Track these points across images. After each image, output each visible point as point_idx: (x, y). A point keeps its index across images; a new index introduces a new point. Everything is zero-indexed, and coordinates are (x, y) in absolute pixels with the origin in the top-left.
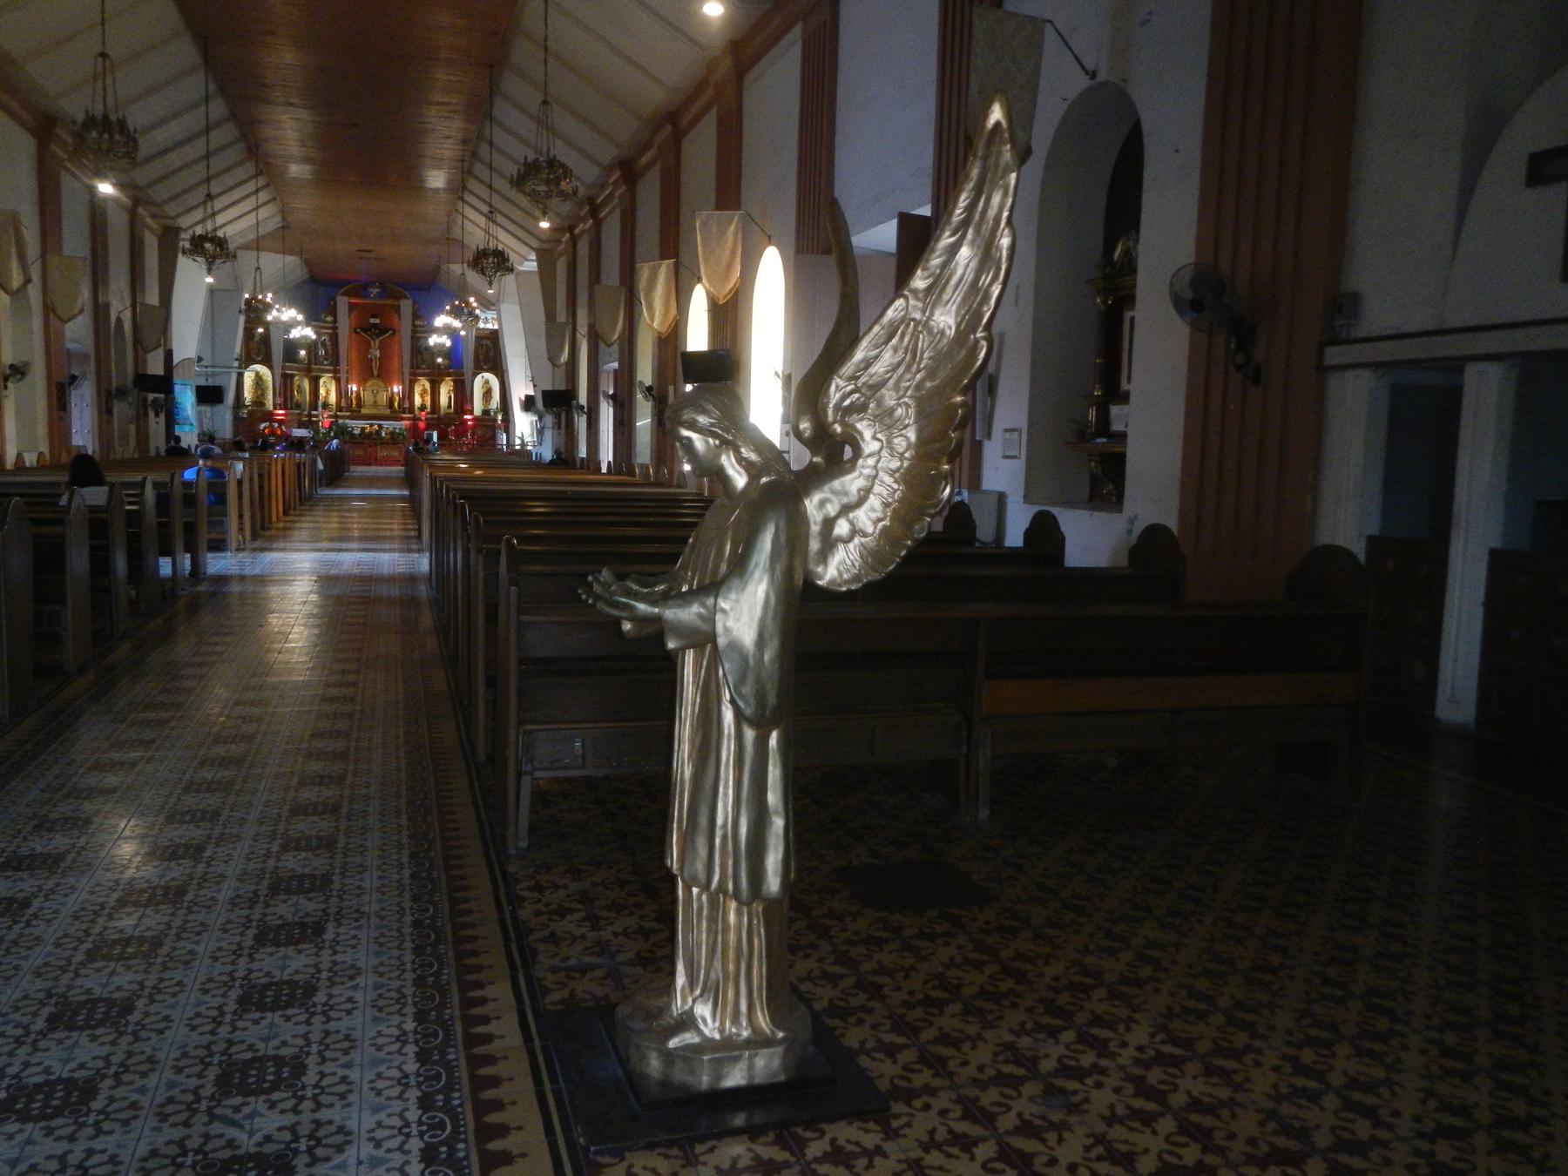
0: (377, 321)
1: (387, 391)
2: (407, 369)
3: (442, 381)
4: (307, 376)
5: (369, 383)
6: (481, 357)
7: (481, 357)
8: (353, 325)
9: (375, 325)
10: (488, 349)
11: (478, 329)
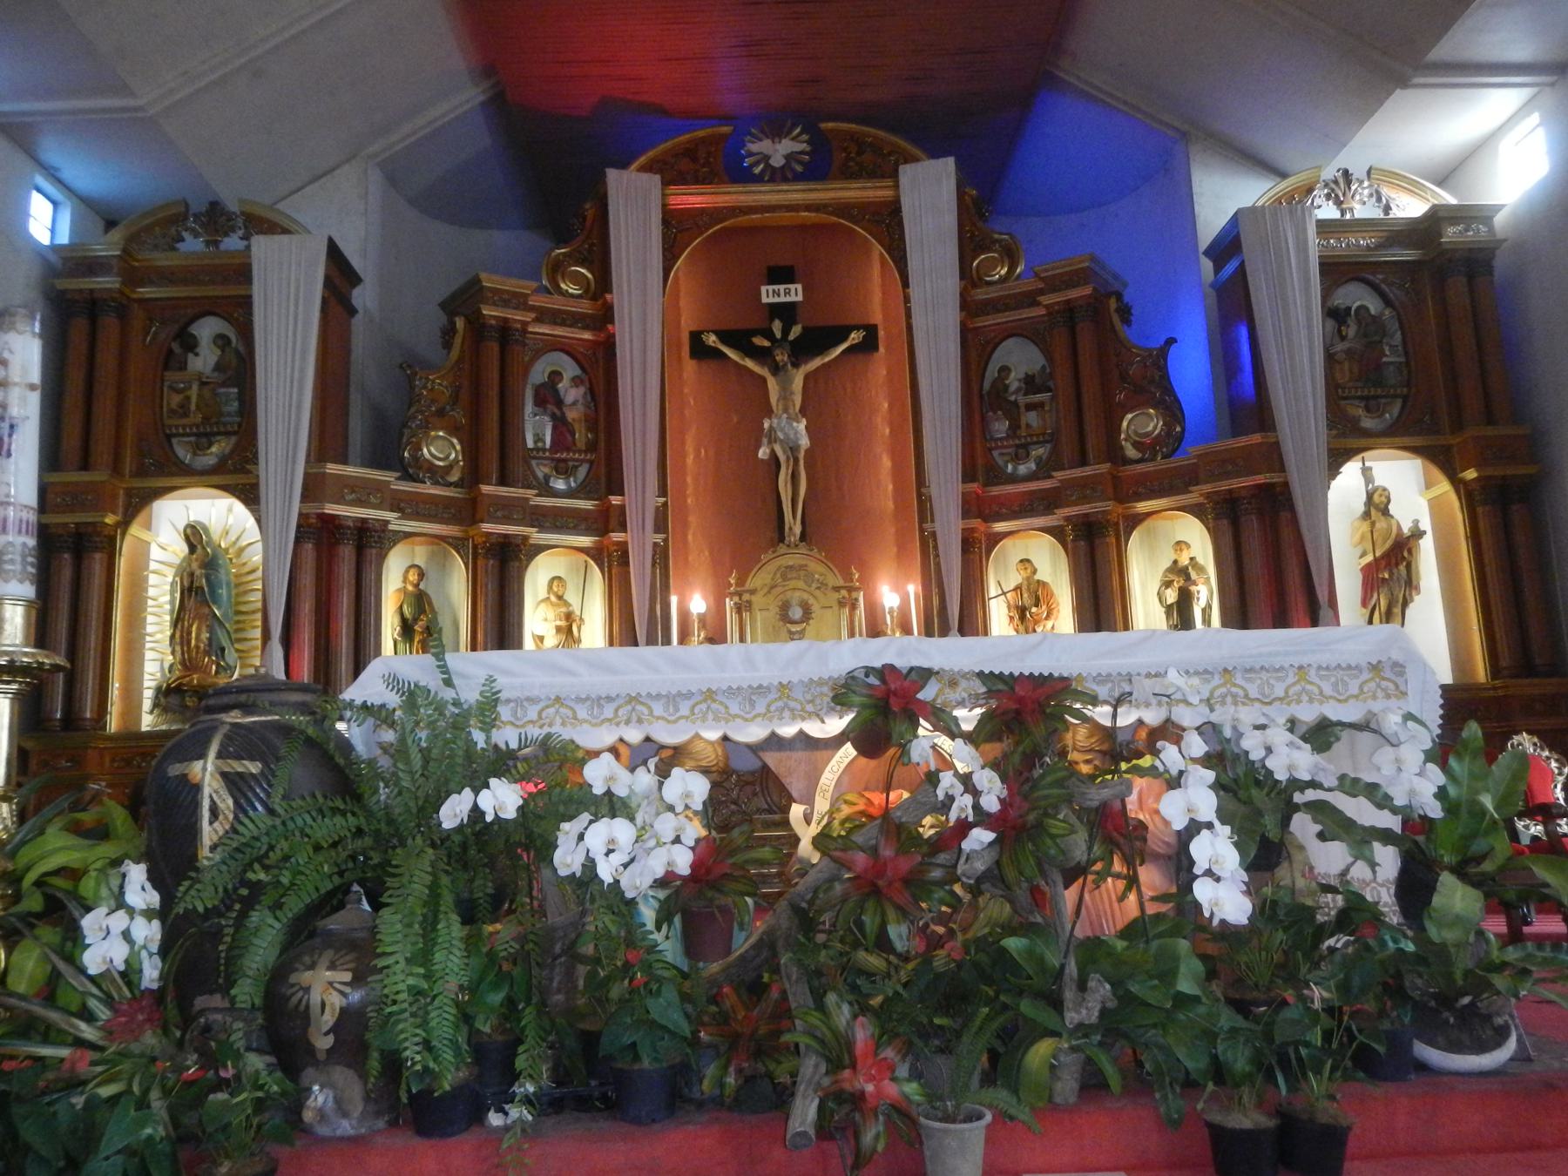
0: (794, 293)
1: (854, 607)
2: (946, 487)
3: (1135, 521)
4: (458, 544)
5: (758, 580)
6: (1343, 376)
8: (687, 324)
9: (786, 312)
10: (1371, 326)
11: (1325, 227)
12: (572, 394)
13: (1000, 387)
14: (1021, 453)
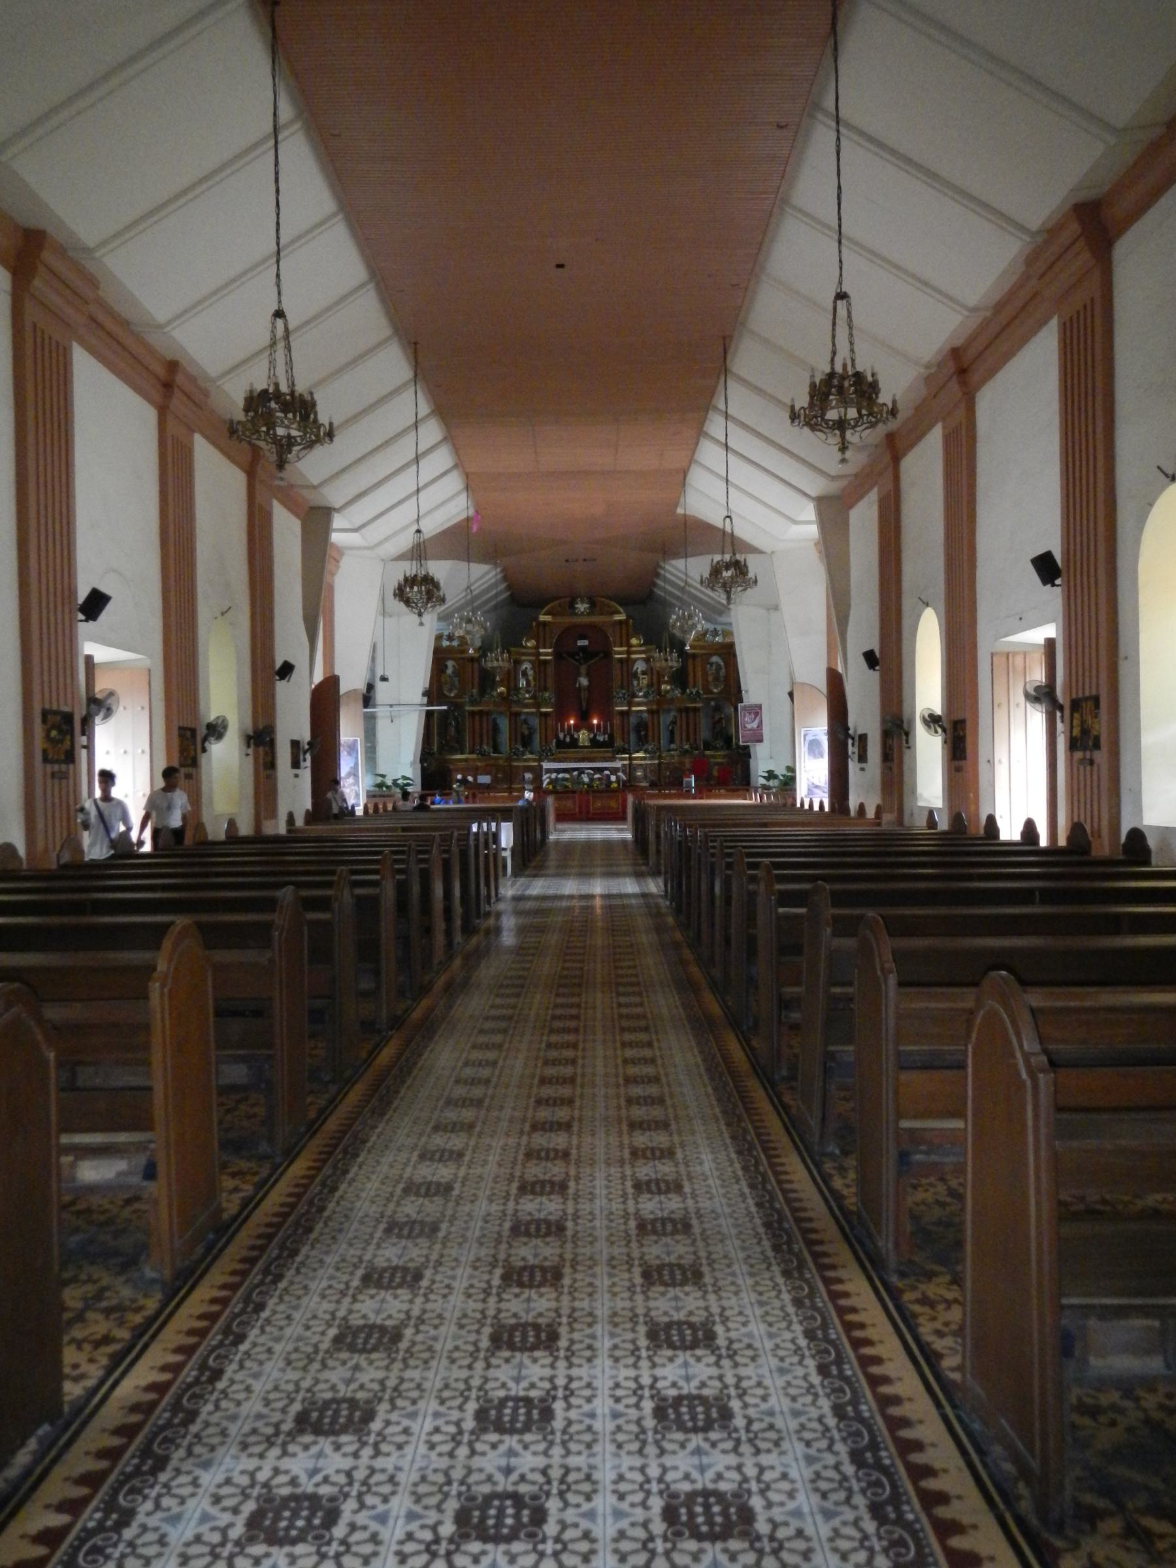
0: (585, 643)
6: (710, 679)
7: (710, 679)
9: (583, 648)
10: (719, 667)
12: (530, 673)
13: (636, 672)
14: (640, 690)
